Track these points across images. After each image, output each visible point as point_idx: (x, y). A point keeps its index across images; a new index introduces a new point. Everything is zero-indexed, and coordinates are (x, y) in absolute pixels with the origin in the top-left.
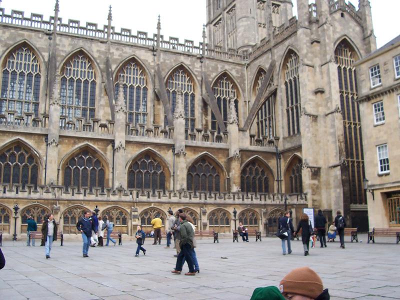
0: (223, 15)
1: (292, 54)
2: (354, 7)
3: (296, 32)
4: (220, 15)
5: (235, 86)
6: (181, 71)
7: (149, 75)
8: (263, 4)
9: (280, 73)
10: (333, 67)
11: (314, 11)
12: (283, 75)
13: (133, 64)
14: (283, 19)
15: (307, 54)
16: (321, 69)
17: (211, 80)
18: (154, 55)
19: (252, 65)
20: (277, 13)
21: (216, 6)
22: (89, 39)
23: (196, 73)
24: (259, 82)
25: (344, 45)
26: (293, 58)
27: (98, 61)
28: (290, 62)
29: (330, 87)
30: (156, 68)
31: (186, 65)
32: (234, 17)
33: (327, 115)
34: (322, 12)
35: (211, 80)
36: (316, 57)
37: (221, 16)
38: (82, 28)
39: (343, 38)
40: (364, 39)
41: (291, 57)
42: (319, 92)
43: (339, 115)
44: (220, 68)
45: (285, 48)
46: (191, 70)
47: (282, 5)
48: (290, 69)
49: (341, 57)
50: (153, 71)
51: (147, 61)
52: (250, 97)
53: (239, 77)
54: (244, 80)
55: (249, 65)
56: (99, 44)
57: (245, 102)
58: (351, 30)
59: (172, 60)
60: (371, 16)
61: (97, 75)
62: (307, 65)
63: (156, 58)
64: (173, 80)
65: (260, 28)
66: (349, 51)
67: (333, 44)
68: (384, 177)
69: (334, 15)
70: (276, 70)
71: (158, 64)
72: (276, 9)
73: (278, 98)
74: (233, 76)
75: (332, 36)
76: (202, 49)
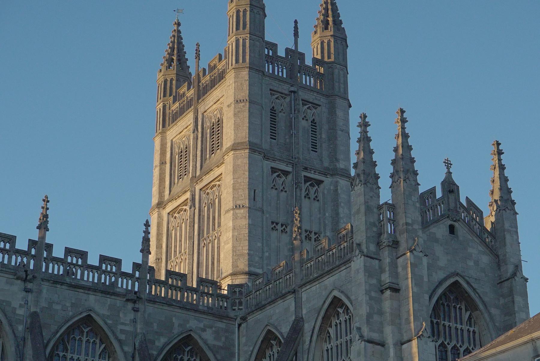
1: (341, 307)
2: (480, 213)
3: (349, 261)
6: (86, 331)
7: (11, 336)
8: (282, 179)
9: (312, 349)
11: (389, 220)
14: (327, 214)
15: (369, 316)
16: (401, 349)
17: (155, 353)
18: (27, 291)
19: (251, 319)
20: (316, 199)
23: (122, 337)
26: (342, 318)
28: (336, 325)
30: (29, 321)
31: (98, 315)
32: (217, 201)
35: (155, 353)
39: (452, 280)
41: (338, 314)
44: (176, 325)
45: (325, 293)
46: (109, 327)
47: (327, 181)
48: (334, 343)
49: (447, 323)
50: (20, 328)
51: (9, 303)
58: (471, 263)
59: (68, 304)
60: (517, 232)
62: (370, 341)
63: (30, 297)
64: (67, 352)
65: (274, 234)
66: (466, 310)
67: (427, 297)
69: (433, 229)
70: (304, 342)
71: (35, 312)
72: (312, 190)
74: (205, 342)
75: (426, 279)
76: (138, 279)
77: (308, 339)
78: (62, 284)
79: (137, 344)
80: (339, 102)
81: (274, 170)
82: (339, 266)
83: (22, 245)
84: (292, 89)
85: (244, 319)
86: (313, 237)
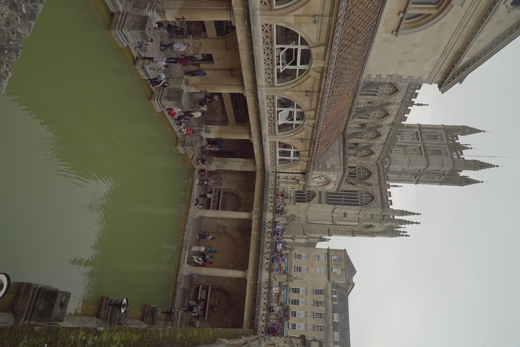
0: (419, 143)
4: (422, 140)
5: (365, 156)
7: (377, 121)
10: (357, 224)
12: (362, 190)
13: (385, 113)
19: (376, 167)
21: (432, 134)
22: (406, 95)
23: (375, 141)
24: (364, 171)
25: (371, 226)
27: (389, 99)
28: (368, 196)
29: (346, 221)
33: (332, 217)
34: (388, 222)
36: (364, 216)
37: (420, 141)
38: (415, 91)
40: (372, 232)
42: (345, 215)
43: (331, 223)
47: (416, 180)
50: (379, 123)
51: (386, 121)
52: (357, 163)
53: (370, 159)
54: (368, 161)
55: (377, 164)
56: (401, 100)
57: (355, 160)
61: (380, 97)
68: (294, 256)
70: (366, 186)
73: (350, 185)
77: (366, 188)
78: (391, 131)
79: (372, 145)
80: (440, 184)
81: (420, 170)
82: (382, 201)
83: (403, 123)
84: (445, 175)
85: (377, 164)
86: (400, 176)
